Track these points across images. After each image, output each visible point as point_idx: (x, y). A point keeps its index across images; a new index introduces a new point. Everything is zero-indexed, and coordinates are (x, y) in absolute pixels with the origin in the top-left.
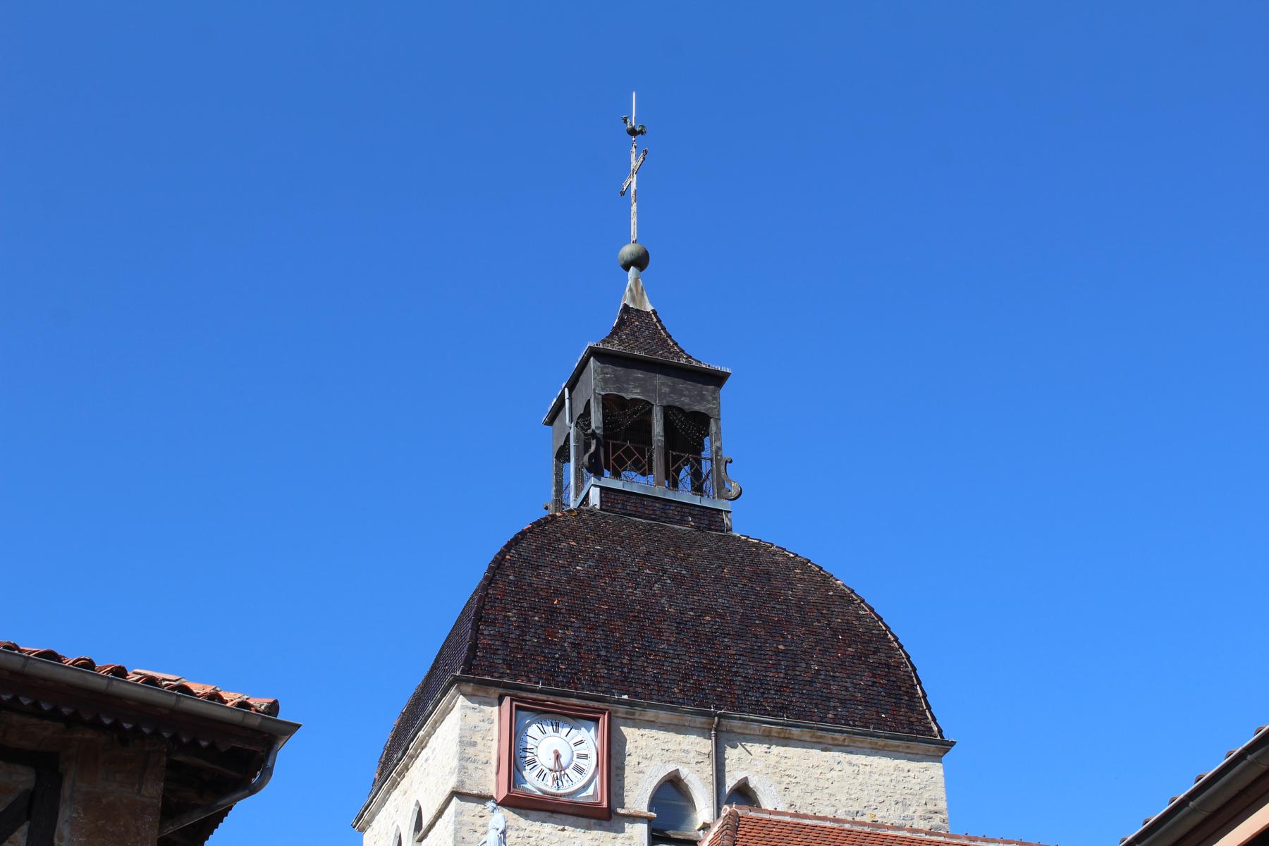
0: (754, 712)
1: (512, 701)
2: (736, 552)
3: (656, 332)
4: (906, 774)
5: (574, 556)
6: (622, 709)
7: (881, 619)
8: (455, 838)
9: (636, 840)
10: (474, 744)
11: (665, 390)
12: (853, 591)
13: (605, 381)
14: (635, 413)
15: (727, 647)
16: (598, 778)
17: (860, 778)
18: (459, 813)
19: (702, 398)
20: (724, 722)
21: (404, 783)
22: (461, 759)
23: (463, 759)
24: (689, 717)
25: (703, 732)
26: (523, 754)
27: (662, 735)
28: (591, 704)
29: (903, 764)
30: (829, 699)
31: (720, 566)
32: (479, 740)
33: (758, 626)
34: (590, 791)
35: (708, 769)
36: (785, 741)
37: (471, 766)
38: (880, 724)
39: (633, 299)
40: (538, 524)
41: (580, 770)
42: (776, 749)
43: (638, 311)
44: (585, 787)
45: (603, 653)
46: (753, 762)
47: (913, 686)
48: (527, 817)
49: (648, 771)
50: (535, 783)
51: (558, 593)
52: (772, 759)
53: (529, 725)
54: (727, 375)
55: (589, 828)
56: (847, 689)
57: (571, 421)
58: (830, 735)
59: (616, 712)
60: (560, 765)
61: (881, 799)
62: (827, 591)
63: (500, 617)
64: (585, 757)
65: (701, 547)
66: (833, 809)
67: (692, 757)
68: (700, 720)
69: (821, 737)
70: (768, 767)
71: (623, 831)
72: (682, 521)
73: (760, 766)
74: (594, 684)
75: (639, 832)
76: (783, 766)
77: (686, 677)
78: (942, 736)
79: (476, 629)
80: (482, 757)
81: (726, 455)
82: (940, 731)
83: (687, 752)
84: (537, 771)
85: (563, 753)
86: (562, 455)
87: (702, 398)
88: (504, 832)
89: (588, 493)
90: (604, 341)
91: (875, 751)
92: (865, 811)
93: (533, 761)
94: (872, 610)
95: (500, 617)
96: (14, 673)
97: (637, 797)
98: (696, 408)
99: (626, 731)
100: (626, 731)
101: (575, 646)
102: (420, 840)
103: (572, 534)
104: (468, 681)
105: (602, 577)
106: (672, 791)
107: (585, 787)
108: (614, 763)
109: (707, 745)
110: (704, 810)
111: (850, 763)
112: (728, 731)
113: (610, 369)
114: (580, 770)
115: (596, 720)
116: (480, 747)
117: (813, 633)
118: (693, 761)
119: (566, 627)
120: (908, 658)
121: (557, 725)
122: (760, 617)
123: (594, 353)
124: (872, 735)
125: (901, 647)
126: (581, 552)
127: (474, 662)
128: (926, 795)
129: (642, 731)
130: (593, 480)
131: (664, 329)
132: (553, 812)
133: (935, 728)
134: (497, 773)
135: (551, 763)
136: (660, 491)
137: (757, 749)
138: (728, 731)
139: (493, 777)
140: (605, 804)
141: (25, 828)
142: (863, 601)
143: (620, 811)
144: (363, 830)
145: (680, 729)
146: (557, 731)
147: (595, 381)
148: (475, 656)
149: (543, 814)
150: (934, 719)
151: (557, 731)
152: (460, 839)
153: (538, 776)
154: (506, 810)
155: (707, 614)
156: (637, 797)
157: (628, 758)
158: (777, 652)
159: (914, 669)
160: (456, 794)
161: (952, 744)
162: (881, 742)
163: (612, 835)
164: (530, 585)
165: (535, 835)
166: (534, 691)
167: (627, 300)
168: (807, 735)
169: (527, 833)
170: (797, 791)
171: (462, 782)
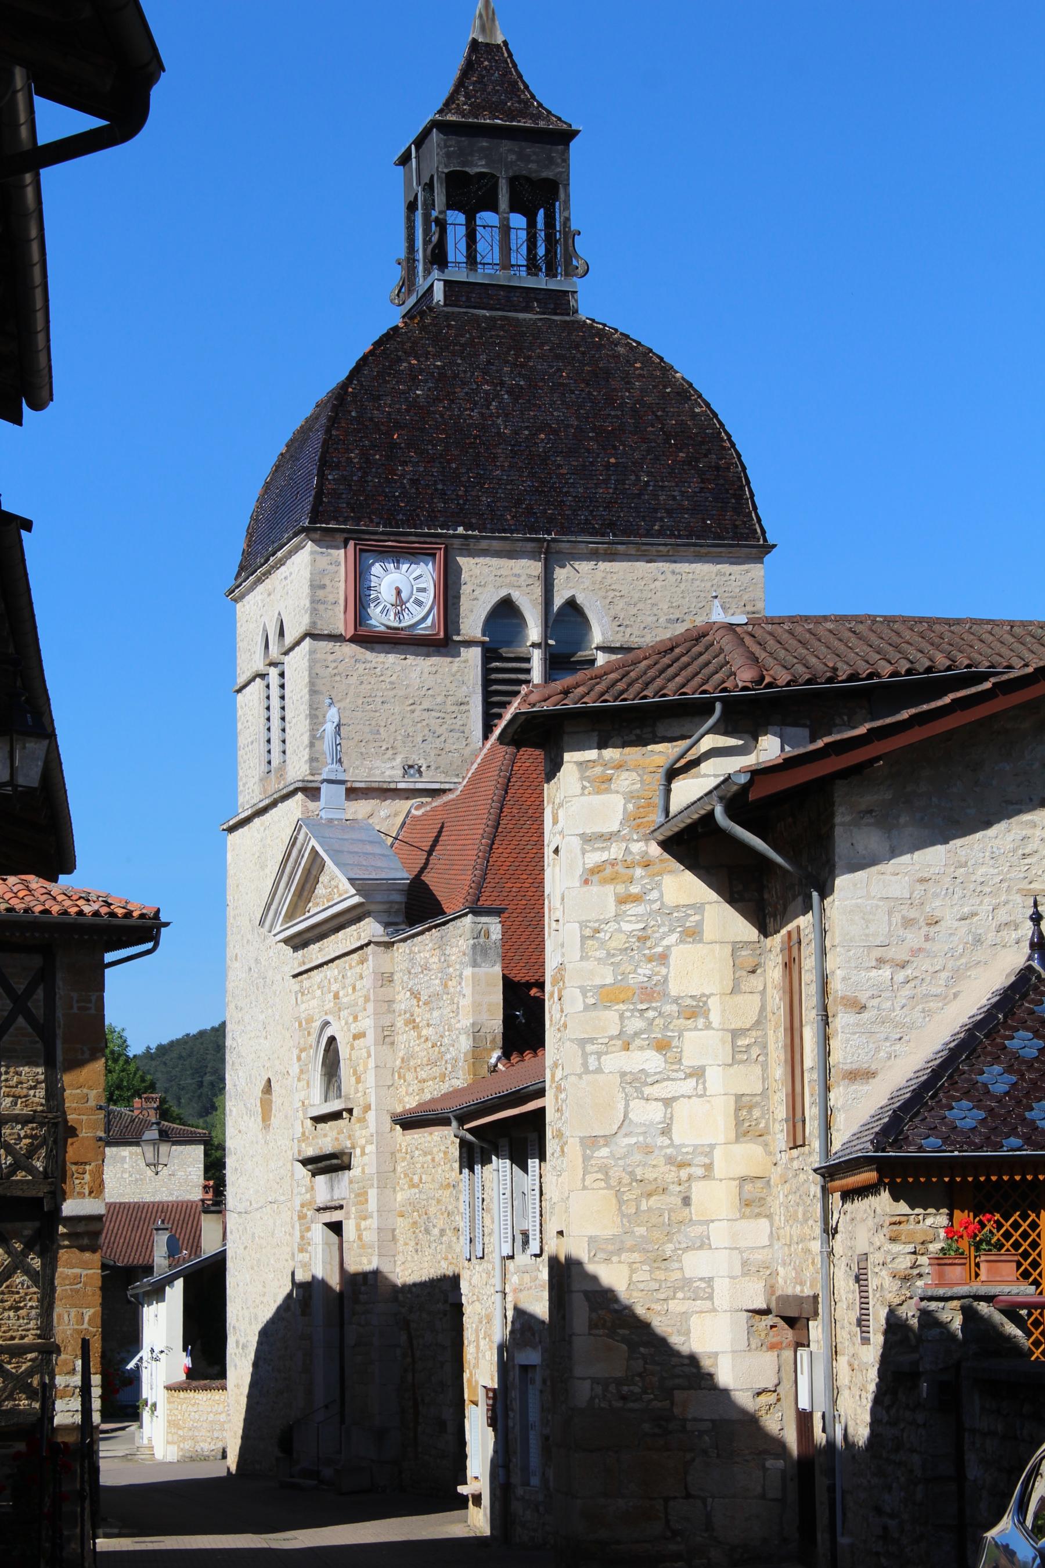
0: (583, 532)
1: (356, 545)
2: (577, 347)
3: (507, 72)
4: (727, 578)
5: (414, 378)
6: (457, 542)
7: (716, 415)
8: (310, 674)
9: (470, 662)
10: (324, 587)
11: (512, 157)
12: (691, 385)
13: (448, 155)
14: (479, 189)
15: (559, 466)
16: (435, 610)
17: (683, 586)
18: (312, 652)
19: (551, 161)
20: (553, 545)
21: (268, 584)
22: (312, 602)
23: (315, 601)
24: (520, 544)
25: (533, 556)
26: (367, 593)
27: (495, 562)
28: (428, 540)
29: (726, 568)
30: (656, 510)
31: (559, 370)
32: (327, 582)
33: (591, 439)
34: (429, 622)
35: (538, 591)
36: (611, 556)
37: (321, 607)
38: (703, 533)
39: (483, 29)
40: (377, 344)
41: (419, 603)
42: (603, 566)
43: (487, 45)
44: (424, 619)
45: (440, 487)
46: (582, 580)
47: (742, 488)
48: (372, 650)
49: (482, 598)
50: (380, 618)
51: (399, 426)
52: (599, 575)
53: (373, 564)
54: (577, 132)
55: (428, 655)
56: (674, 498)
57: (419, 183)
58: (654, 548)
59: (452, 544)
60: (401, 599)
61: (701, 605)
62: (665, 387)
63: (343, 460)
64: (424, 590)
65: (543, 344)
66: (655, 618)
67: (523, 581)
68: (530, 546)
69: (645, 551)
70: (594, 583)
71: (459, 655)
72: (527, 309)
73: (587, 583)
74: (432, 522)
75: (473, 656)
76: (608, 581)
77: (519, 502)
78: (765, 540)
79: (321, 475)
80: (331, 598)
81: (574, 226)
82: (763, 532)
83: (519, 576)
84: (380, 608)
85: (404, 588)
86: (412, 207)
87: (551, 161)
88: (339, 725)
89: (432, 285)
90: (447, 104)
91: (699, 558)
92: (686, 617)
93: (377, 598)
94: (708, 405)
95: (343, 460)
96: (29, 922)
97: (472, 622)
98: (544, 174)
99: (461, 560)
100: (461, 560)
101: (413, 482)
102: (286, 653)
103: (413, 352)
104: (316, 529)
105: (441, 401)
106: (506, 611)
107: (424, 619)
108: (450, 593)
109: (536, 567)
110: (534, 632)
111: (673, 572)
112: (557, 552)
113: (453, 140)
114: (419, 603)
115: (434, 555)
116: (329, 589)
117: (644, 440)
118: (524, 584)
119: (404, 463)
120: (739, 456)
121: (398, 562)
122: (593, 430)
123: (434, 124)
124: (695, 545)
125: (733, 445)
126: (421, 371)
127: (321, 509)
128: (746, 597)
129: (477, 560)
130: (436, 273)
131: (515, 66)
132: (395, 644)
133: (759, 530)
134: (345, 612)
135: (393, 599)
136: (502, 278)
137: (585, 566)
138: (557, 552)
139: (342, 616)
140: (442, 635)
141: (41, 987)
142: (700, 396)
143: (456, 638)
144: (236, 600)
145: (511, 555)
146: (398, 568)
147: (436, 160)
148: (322, 502)
149: (387, 646)
150: (759, 520)
151: (398, 568)
152: (314, 675)
153: (382, 612)
154: (353, 646)
155: (542, 431)
156: (472, 622)
157: (463, 587)
158: (608, 466)
159: (744, 469)
160: (308, 635)
161: (774, 546)
162: (703, 550)
163: (449, 659)
164: (371, 419)
165: (380, 667)
166: (375, 533)
167: (475, 34)
168: (632, 550)
169: (373, 665)
170: (621, 604)
171: (313, 624)
